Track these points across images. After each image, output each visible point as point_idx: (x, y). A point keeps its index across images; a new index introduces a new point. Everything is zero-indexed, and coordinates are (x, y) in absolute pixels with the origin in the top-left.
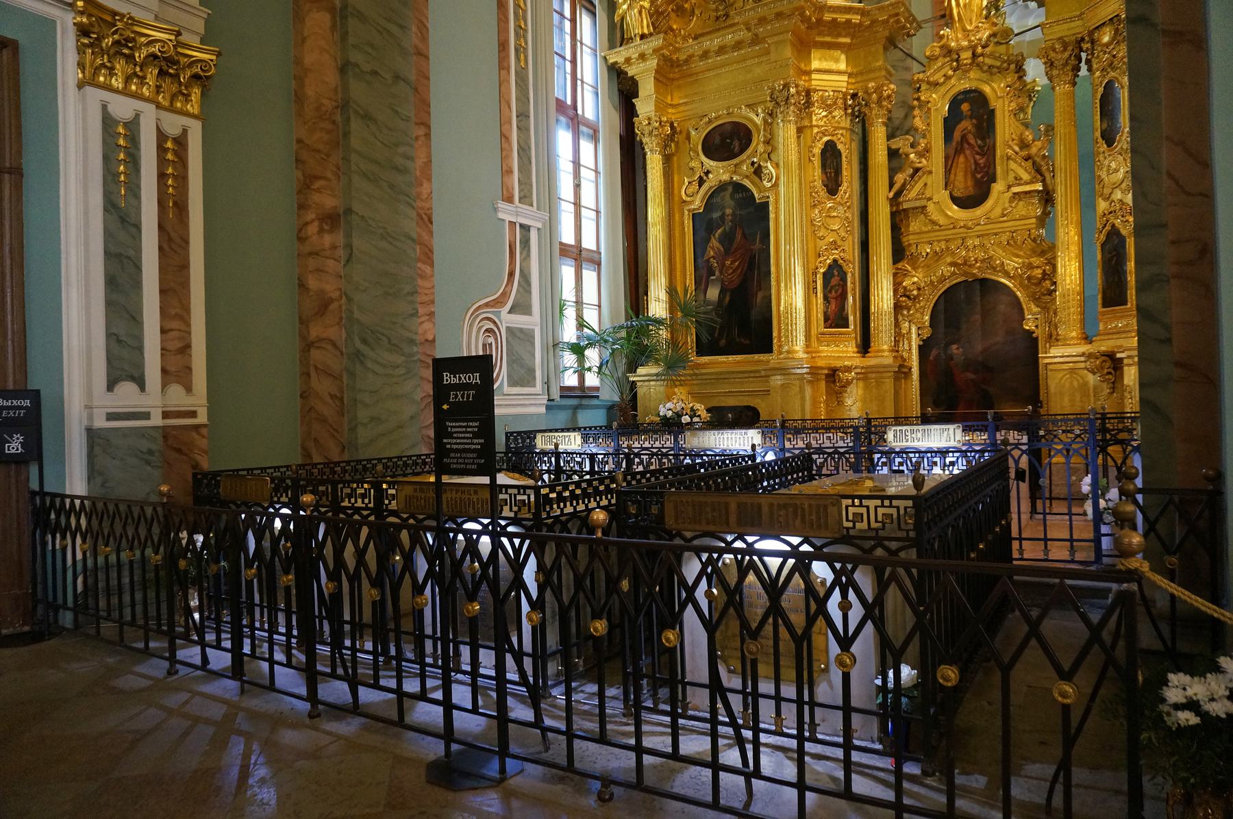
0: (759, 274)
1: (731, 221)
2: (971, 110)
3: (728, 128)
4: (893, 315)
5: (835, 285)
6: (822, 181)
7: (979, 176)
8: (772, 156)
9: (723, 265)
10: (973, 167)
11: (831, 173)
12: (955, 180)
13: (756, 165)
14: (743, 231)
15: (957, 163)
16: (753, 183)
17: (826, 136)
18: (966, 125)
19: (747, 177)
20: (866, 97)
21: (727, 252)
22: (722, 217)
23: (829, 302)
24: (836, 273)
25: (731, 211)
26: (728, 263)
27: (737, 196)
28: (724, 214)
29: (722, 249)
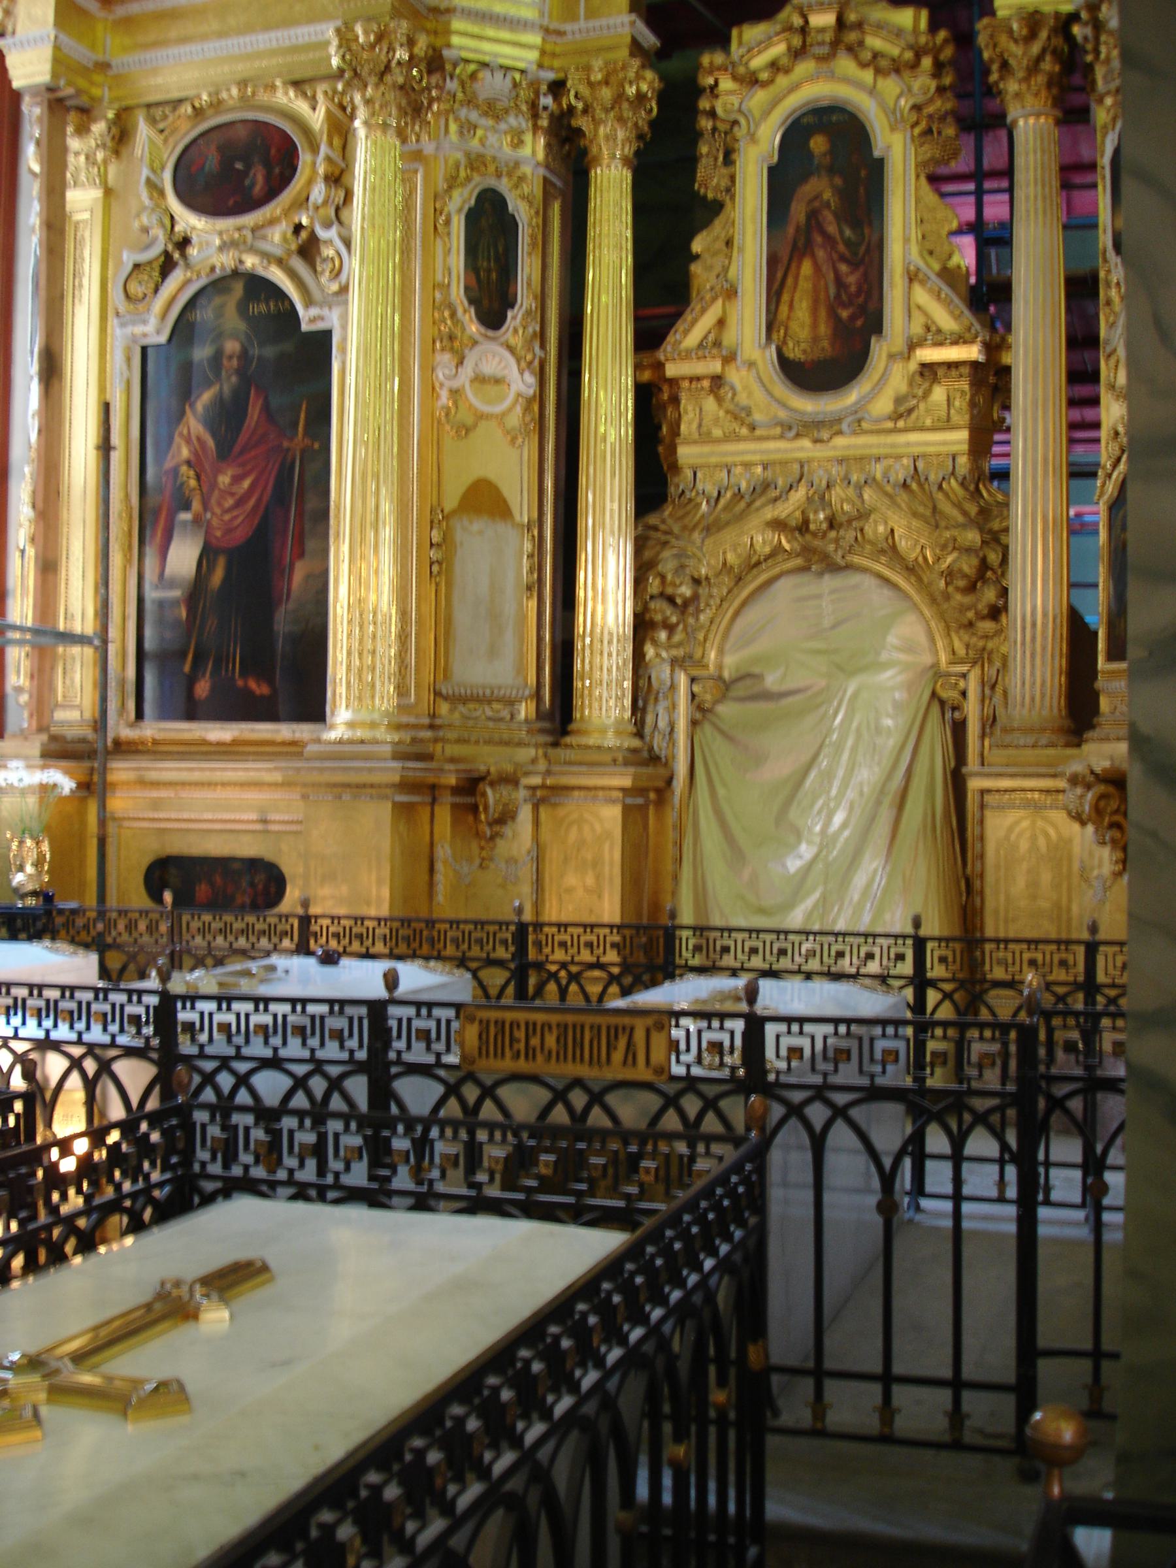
0: (300, 514)
3: (242, 132)
6: (467, 289)
7: (845, 314)
8: (344, 214)
9: (214, 485)
10: (832, 291)
11: (489, 271)
12: (789, 318)
13: (304, 235)
16: (293, 275)
20: (585, 91)
21: (225, 451)
22: (217, 359)
26: (224, 480)
27: (259, 308)
29: (211, 443)
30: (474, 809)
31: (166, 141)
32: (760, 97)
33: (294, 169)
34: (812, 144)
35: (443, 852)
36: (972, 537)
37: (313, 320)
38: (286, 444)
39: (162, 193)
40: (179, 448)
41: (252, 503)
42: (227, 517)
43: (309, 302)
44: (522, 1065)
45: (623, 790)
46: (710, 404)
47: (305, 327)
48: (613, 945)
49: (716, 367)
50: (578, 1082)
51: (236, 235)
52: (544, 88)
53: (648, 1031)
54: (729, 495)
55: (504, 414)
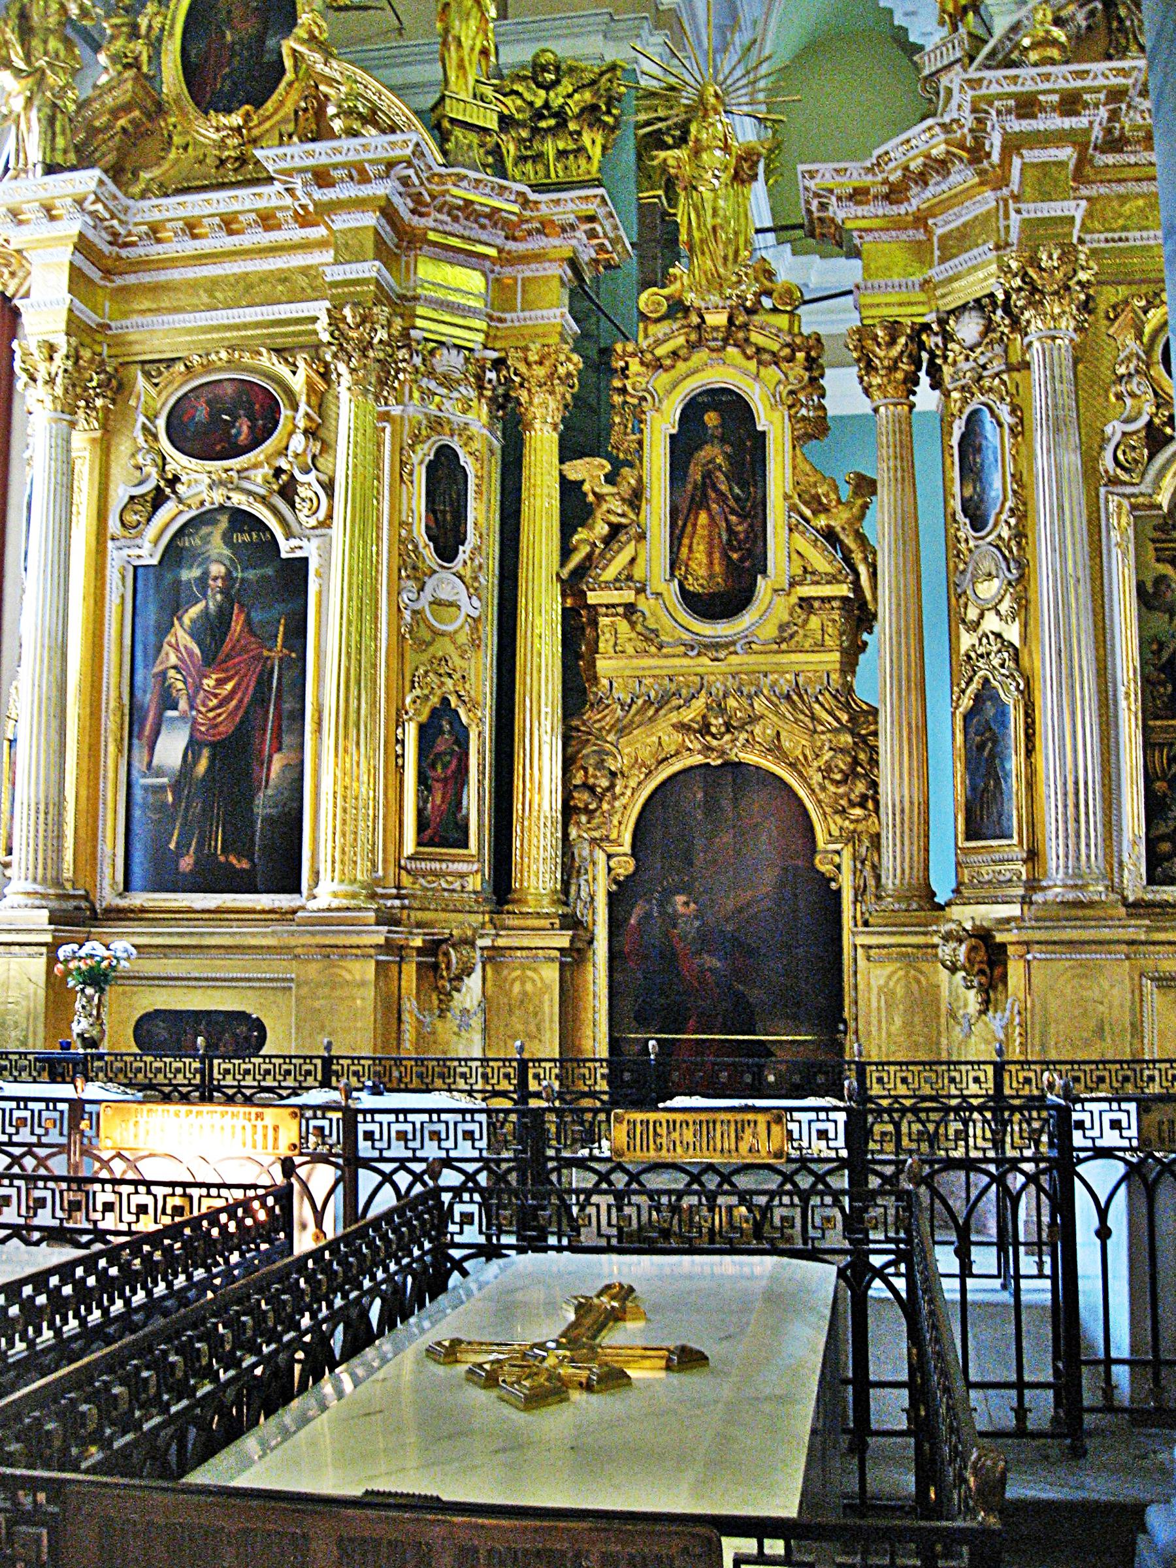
1: (221, 592)
2: (722, 425)
4: (559, 826)
5: (445, 754)
6: (427, 527)
7: (735, 556)
9: (199, 687)
10: (725, 537)
14: (248, 615)
15: (694, 525)
18: (713, 453)
21: (211, 659)
22: (203, 580)
23: (429, 789)
24: (447, 727)
25: (223, 570)
26: (208, 683)
27: (239, 538)
28: (206, 574)
29: (197, 651)
30: (435, 967)
31: (159, 394)
32: (663, 379)
33: (276, 423)
34: (706, 418)
35: (410, 1005)
36: (847, 739)
37: (292, 550)
38: (266, 653)
39: (155, 437)
41: (234, 703)
42: (211, 715)
43: (289, 535)
44: (666, 1156)
45: (561, 950)
46: (623, 626)
47: (284, 555)
48: (603, 1076)
49: (628, 596)
50: (711, 1167)
51: (224, 476)
52: (488, 365)
53: (769, 1123)
54: (640, 702)
55: (456, 632)
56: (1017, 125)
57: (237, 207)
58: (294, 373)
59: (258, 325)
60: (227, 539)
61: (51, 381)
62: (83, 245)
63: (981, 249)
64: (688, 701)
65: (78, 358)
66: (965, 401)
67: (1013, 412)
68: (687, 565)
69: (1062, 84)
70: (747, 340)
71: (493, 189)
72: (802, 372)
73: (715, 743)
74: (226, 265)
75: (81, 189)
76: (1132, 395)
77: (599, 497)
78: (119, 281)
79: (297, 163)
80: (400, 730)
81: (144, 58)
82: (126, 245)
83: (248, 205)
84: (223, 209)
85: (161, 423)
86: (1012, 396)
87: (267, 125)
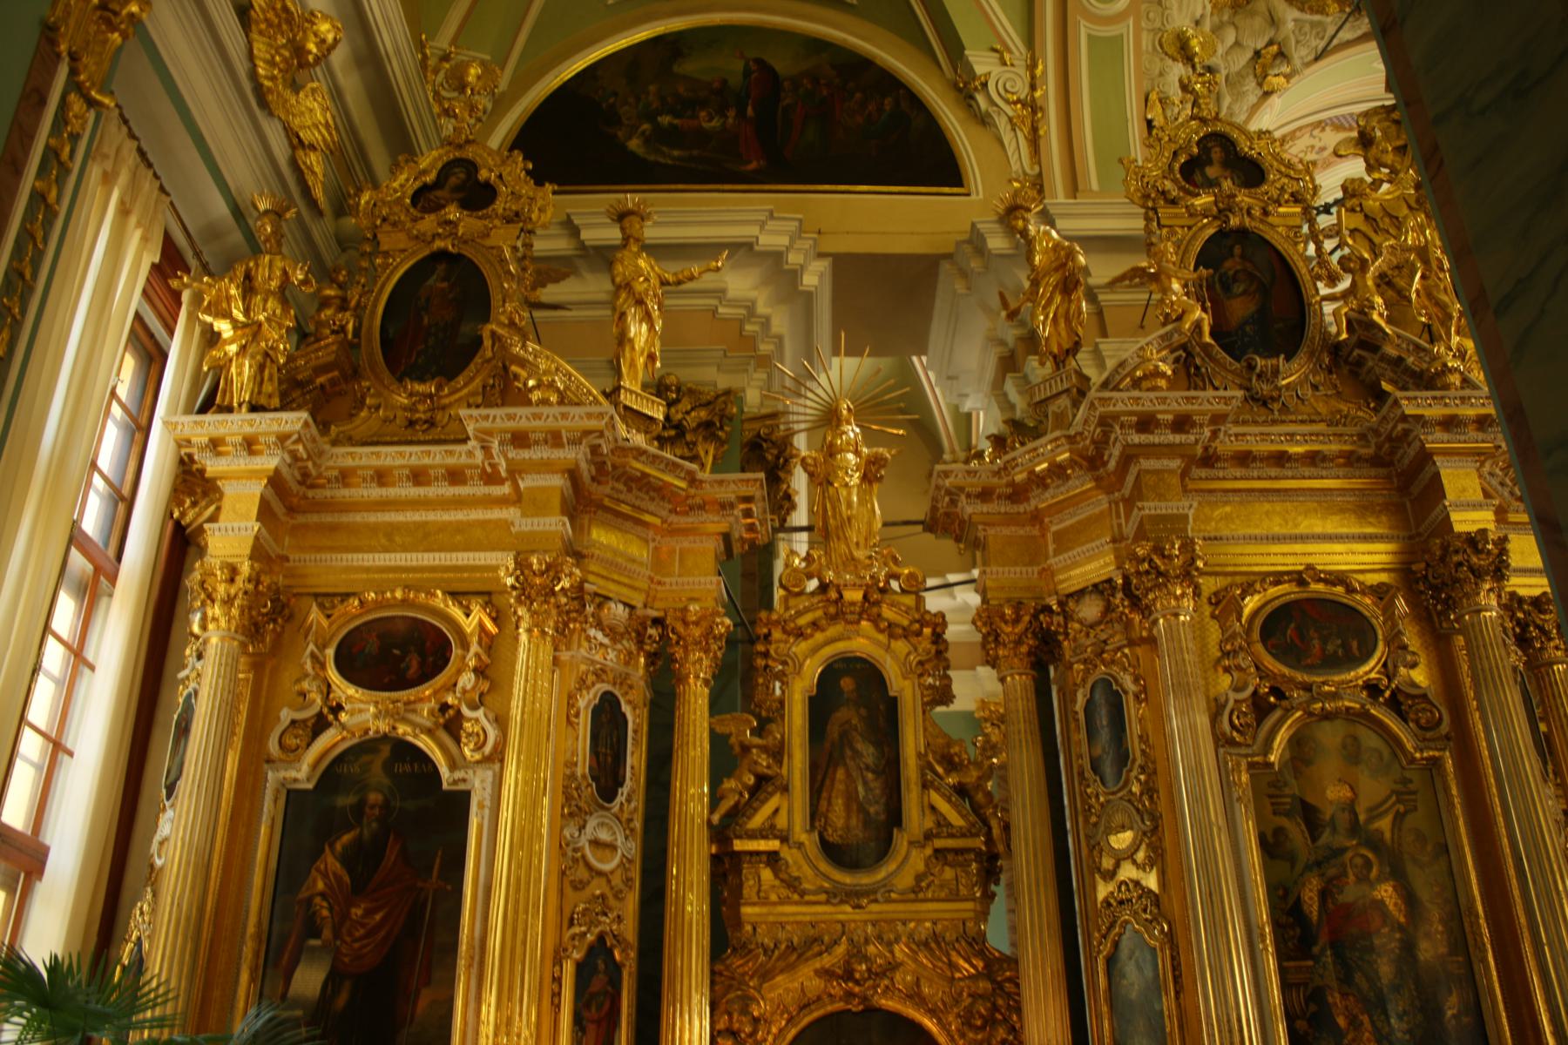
9: (345, 916)
11: (606, 755)
15: (833, 780)
17: (603, 681)
18: (847, 715)
19: (430, 732)
21: (359, 888)
22: (359, 809)
24: (601, 966)
26: (357, 912)
27: (400, 768)
29: (347, 879)
31: (330, 625)
32: (801, 648)
33: (447, 661)
34: (842, 682)
36: (984, 985)
37: (455, 782)
38: (420, 884)
39: (323, 666)
40: (315, 882)
41: (383, 933)
42: (357, 945)
43: (453, 766)
46: (767, 874)
49: (773, 845)
51: (391, 706)
52: (649, 623)
54: (783, 947)
55: (612, 872)
56: (1137, 438)
57: (426, 461)
58: (468, 615)
59: (433, 569)
60: (388, 767)
61: (228, 602)
62: (275, 481)
63: (1098, 543)
64: (828, 949)
65: (258, 582)
66: (1087, 672)
67: (1136, 680)
68: (826, 818)
69: (1175, 406)
70: (879, 615)
71: (667, 465)
72: (929, 646)
73: (857, 989)
74: (408, 514)
75: (287, 428)
76: (1239, 668)
77: (746, 749)
78: (301, 519)
79: (499, 424)
80: (557, 968)
81: (350, 327)
82: (312, 486)
83: (438, 460)
84: (414, 461)
85: (330, 652)
86: (1134, 667)
87: (457, 396)
